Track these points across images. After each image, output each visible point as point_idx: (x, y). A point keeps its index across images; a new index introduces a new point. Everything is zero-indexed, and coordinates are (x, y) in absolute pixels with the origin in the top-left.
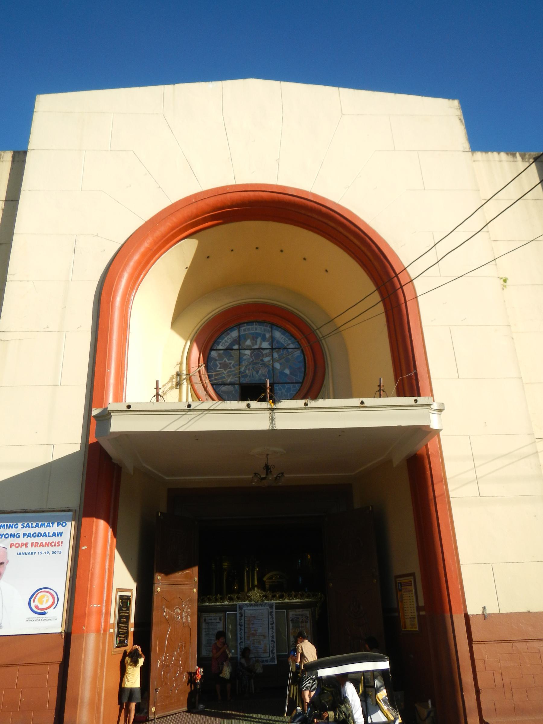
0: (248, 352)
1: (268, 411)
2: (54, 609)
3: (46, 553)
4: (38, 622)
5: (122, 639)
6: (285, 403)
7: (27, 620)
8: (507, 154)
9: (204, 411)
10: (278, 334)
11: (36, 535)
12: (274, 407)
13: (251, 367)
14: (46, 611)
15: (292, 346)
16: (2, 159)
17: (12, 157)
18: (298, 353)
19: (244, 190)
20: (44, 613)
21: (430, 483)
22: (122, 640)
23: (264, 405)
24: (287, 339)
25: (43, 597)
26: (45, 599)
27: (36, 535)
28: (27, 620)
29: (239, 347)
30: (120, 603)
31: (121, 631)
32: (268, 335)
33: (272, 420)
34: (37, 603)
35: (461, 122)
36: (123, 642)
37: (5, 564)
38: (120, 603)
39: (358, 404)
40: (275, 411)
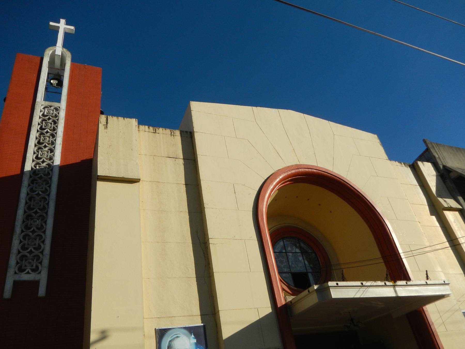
0: (290, 254)
1: (393, 286)
6: (399, 283)
8: (398, 162)
9: (368, 287)
10: (302, 245)
12: (395, 284)
13: (294, 262)
15: (310, 251)
16: (175, 134)
17: (180, 134)
18: (313, 255)
19: (307, 168)
21: (428, 325)
23: (391, 284)
24: (307, 248)
29: (286, 251)
32: (298, 245)
33: (396, 291)
35: (381, 145)
39: (425, 283)
40: (396, 287)
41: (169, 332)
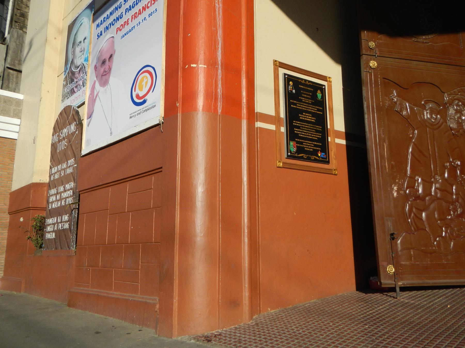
2: (153, 91)
3: (144, 20)
4: (139, 115)
5: (308, 145)
7: (131, 117)
11: (134, 5)
14: (146, 98)
20: (144, 102)
22: (305, 149)
25: (142, 80)
26: (144, 83)
27: (135, 4)
28: (131, 117)
30: (290, 88)
31: (300, 134)
34: (138, 91)
36: (315, 153)
37: (113, 56)
38: (290, 88)
41: (77, 21)
